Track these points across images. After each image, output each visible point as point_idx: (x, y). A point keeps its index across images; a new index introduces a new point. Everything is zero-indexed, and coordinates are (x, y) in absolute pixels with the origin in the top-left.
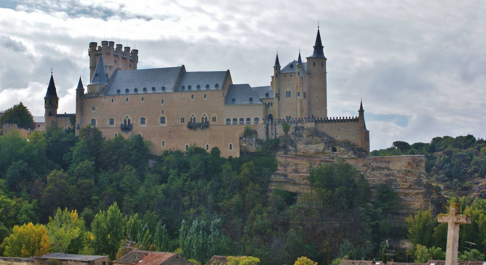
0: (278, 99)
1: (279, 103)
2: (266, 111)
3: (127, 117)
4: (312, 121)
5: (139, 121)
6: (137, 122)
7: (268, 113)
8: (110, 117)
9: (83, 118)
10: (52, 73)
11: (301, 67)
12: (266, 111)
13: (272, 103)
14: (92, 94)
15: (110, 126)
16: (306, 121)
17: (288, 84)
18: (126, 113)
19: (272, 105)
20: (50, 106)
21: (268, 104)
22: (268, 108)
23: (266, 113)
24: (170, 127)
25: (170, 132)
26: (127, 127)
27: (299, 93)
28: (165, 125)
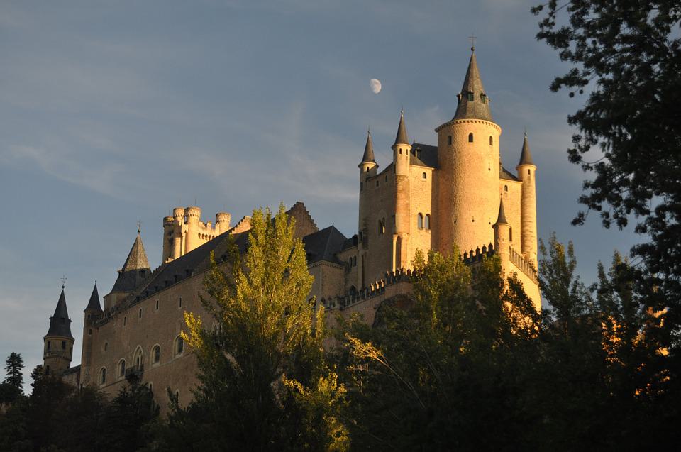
0: (364, 243)
1: (366, 253)
2: (346, 281)
3: (141, 352)
4: (399, 279)
5: (153, 354)
6: (149, 358)
7: (349, 286)
8: (120, 358)
9: (93, 369)
10: (63, 287)
11: (401, 150)
12: (346, 281)
13: (355, 257)
14: (110, 314)
15: (121, 379)
16: (389, 282)
17: (382, 201)
18: (137, 344)
19: (355, 265)
20: (47, 355)
21: (348, 261)
22: (349, 272)
23: (345, 286)
24: (187, 357)
25: (187, 368)
26: (133, 376)
27: (394, 216)
28: (182, 355)
